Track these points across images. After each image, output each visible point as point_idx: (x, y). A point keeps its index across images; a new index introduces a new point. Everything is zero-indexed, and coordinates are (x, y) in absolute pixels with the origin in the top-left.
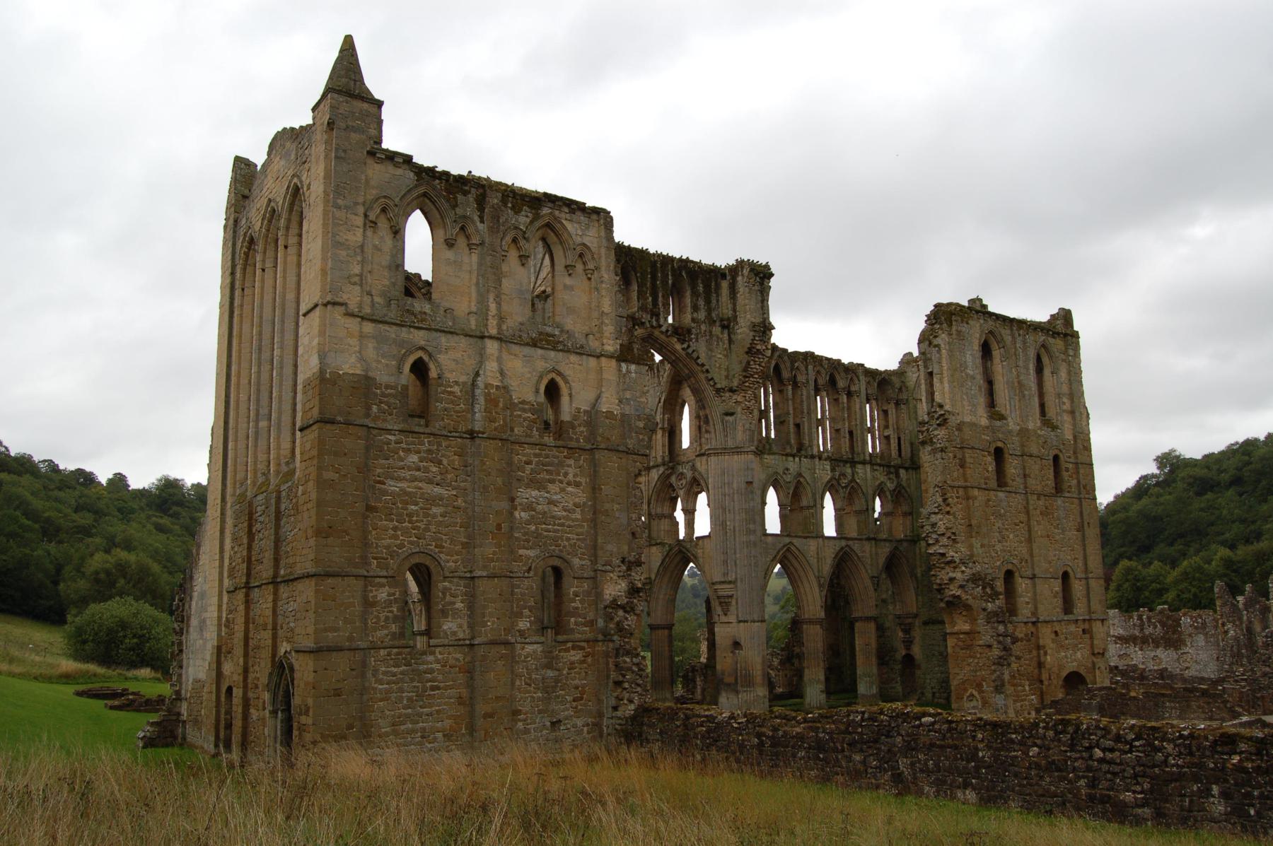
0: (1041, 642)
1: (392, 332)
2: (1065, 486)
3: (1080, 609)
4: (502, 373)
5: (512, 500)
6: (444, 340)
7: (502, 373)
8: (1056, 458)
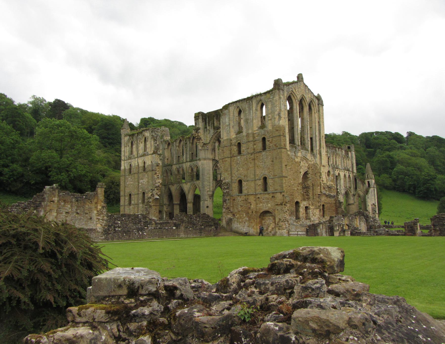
0: (249, 201)
1: (128, 161)
2: (267, 147)
3: (270, 189)
4: (138, 163)
5: (139, 182)
6: (132, 160)
7: (138, 163)
8: (264, 139)
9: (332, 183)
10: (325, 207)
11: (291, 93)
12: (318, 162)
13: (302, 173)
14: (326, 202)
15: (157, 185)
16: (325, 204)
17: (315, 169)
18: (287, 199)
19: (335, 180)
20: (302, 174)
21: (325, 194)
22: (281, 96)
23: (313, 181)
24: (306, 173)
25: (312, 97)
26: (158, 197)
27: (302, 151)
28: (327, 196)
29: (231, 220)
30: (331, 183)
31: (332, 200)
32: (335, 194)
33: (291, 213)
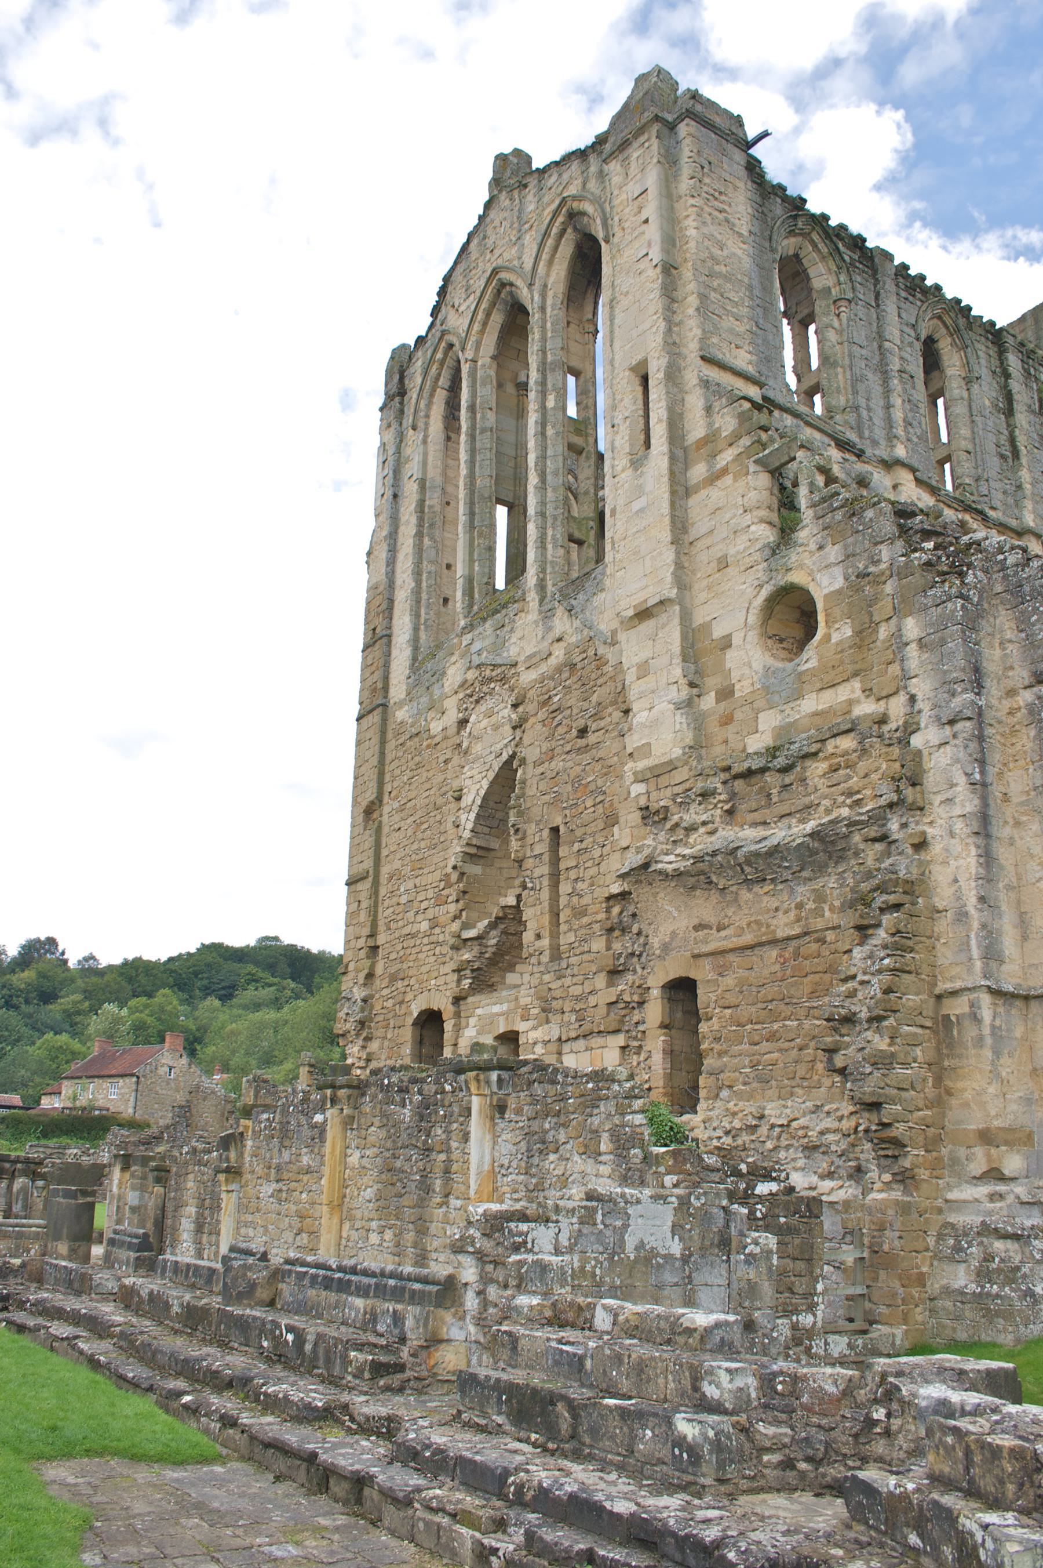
16: (702, 973)
20: (467, 800)
24: (506, 779)
28: (699, 876)
30: (810, 704)
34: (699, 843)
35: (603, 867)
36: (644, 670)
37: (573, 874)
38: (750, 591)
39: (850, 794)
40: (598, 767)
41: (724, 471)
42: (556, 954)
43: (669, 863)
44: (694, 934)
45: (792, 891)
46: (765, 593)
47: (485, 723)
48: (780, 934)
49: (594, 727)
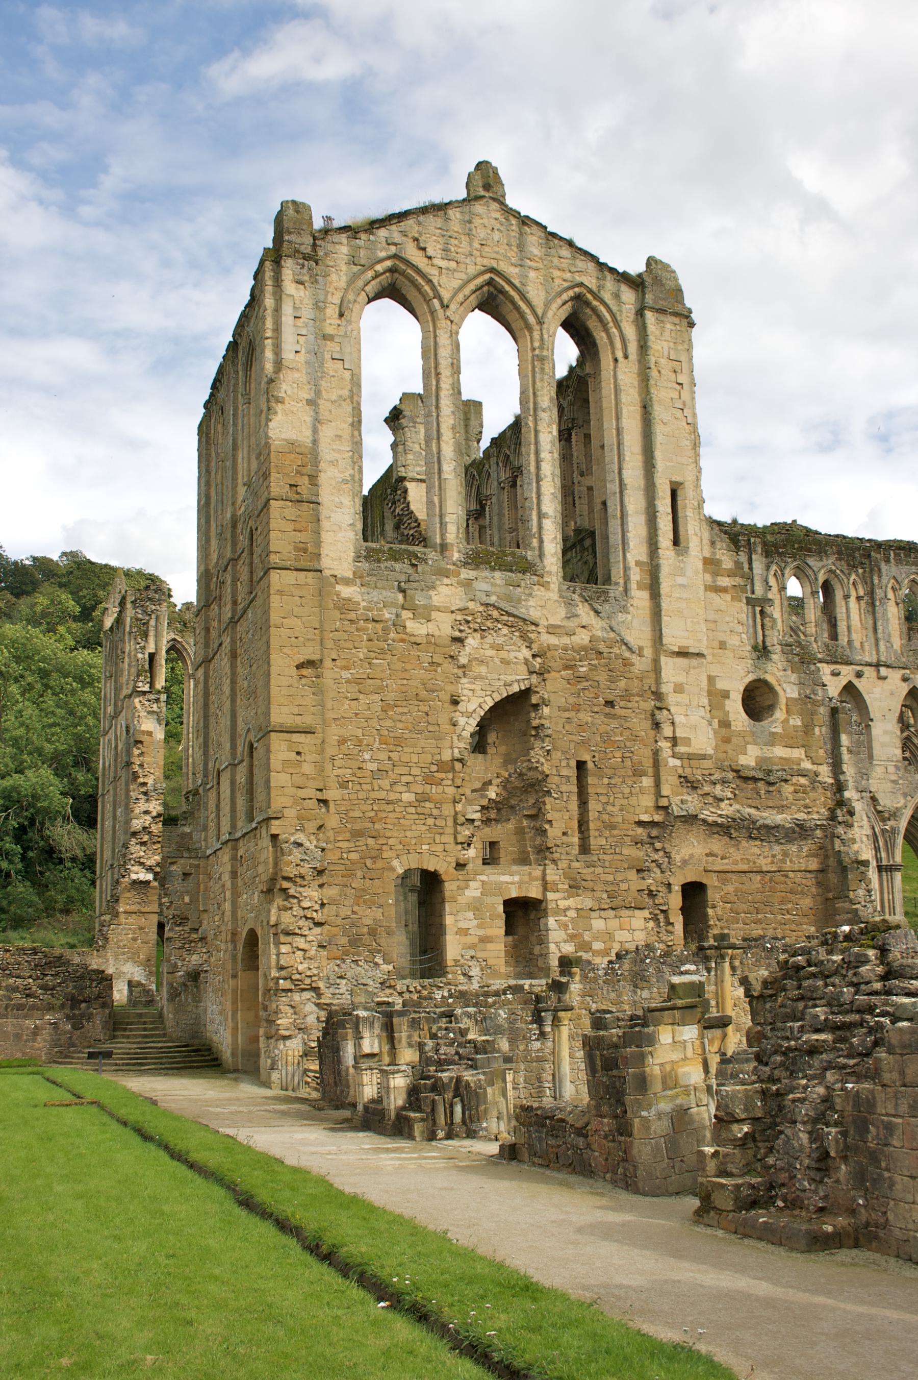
9: (797, 753)
10: (713, 895)
11: (392, 270)
12: (637, 631)
13: (477, 702)
14: (719, 865)
15: (137, 824)
16: (711, 881)
17: (602, 677)
18: (296, 855)
19: (821, 732)
21: (690, 819)
22: (289, 287)
23: (584, 743)
25: (591, 281)
26: (150, 877)
27: (466, 574)
28: (724, 829)
29: (195, 976)
30: (779, 752)
31: (800, 858)
32: (818, 815)
33: (354, 942)
34: (727, 809)
35: (633, 801)
36: (679, 689)
37: (603, 799)
38: (743, 673)
39: (806, 807)
40: (627, 733)
41: (724, 590)
42: (585, 848)
43: (708, 814)
44: (705, 858)
45: (771, 848)
46: (751, 677)
47: (491, 653)
48: (765, 869)
49: (622, 704)
